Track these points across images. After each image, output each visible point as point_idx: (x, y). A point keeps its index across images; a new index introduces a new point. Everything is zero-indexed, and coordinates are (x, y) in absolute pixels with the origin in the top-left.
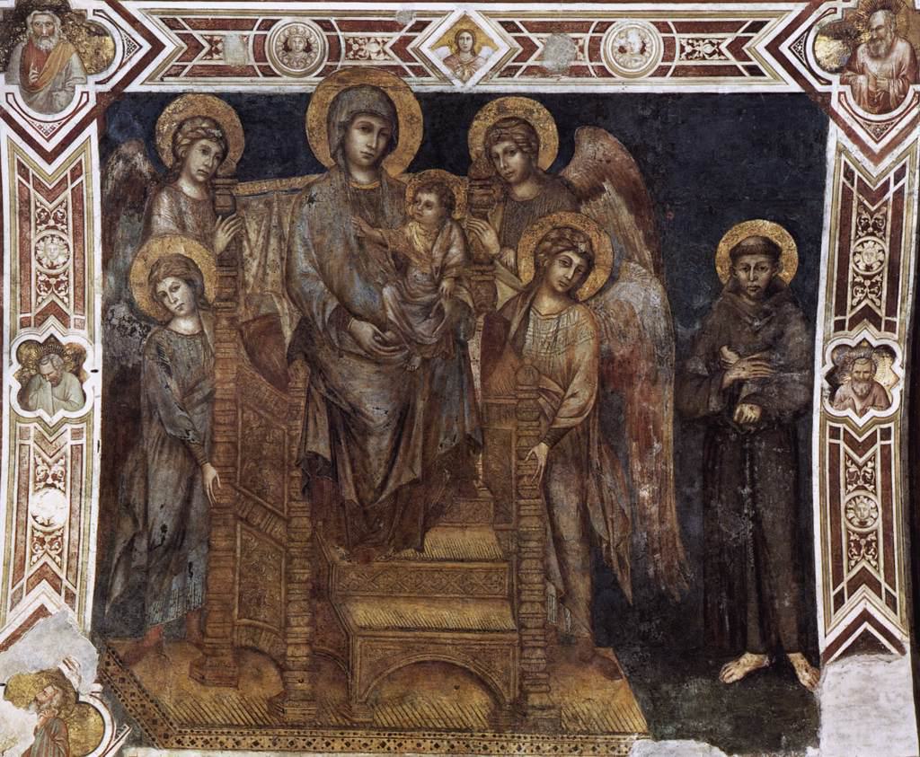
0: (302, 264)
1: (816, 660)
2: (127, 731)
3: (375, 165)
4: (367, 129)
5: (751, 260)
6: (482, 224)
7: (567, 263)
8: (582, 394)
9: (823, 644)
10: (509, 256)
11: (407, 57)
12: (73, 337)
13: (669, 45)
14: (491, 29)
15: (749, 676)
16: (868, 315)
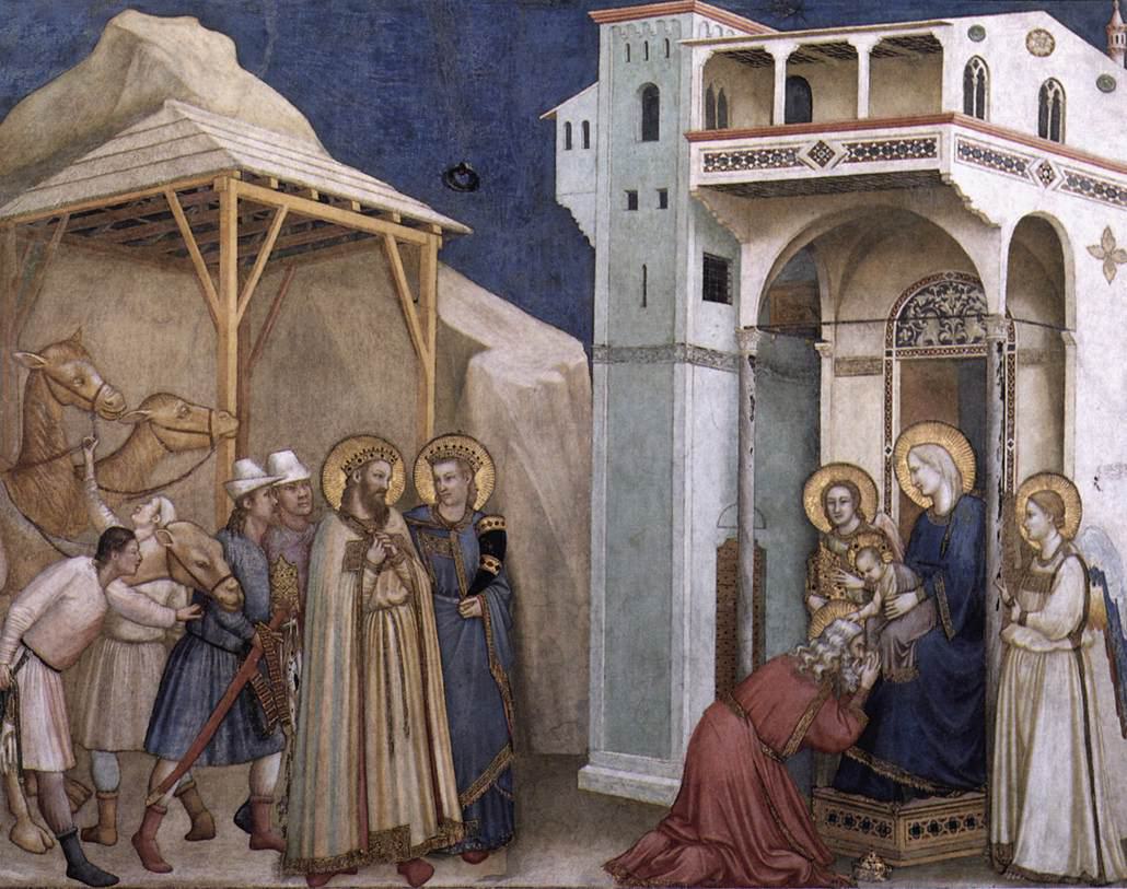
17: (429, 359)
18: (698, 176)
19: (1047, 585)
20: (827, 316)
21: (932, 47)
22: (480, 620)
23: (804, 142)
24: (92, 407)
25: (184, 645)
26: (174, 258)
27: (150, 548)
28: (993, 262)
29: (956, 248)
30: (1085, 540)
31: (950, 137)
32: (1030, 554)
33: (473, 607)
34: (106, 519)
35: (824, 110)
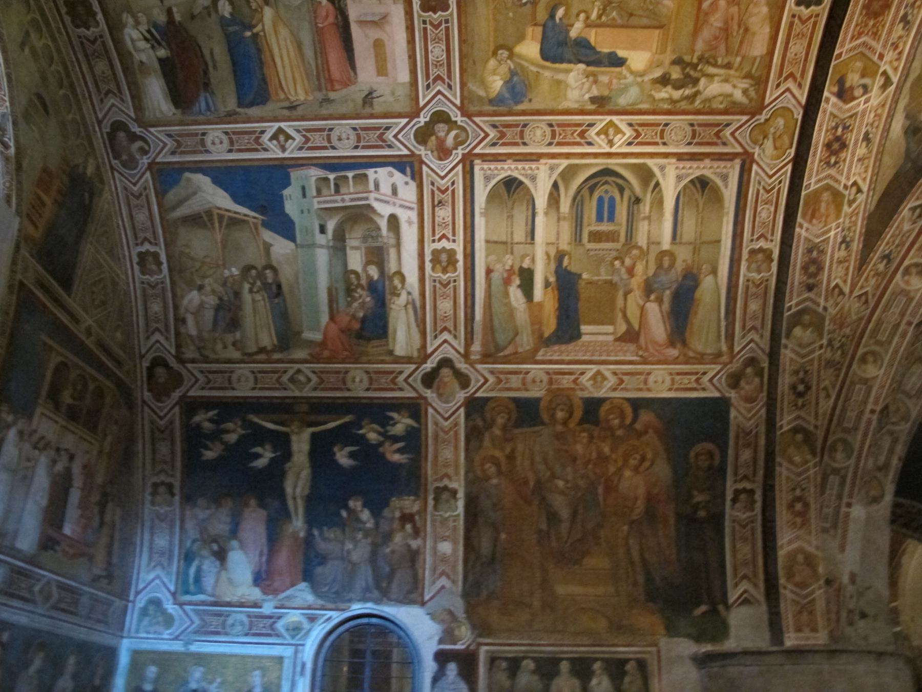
0: (538, 458)
1: (728, 607)
2: (476, 632)
3: (565, 423)
4: (562, 410)
5: (703, 457)
6: (603, 444)
7: (635, 459)
8: (640, 506)
9: (731, 601)
10: (614, 456)
11: (577, 384)
12: (453, 485)
13: (673, 380)
14: (608, 374)
15: (704, 614)
16: (745, 477)
17: (261, 247)
18: (316, 206)
19: (398, 295)
20: (347, 237)
21: (365, 176)
22: (278, 303)
23: (338, 198)
24: (192, 259)
25: (218, 308)
26: (203, 226)
27: (208, 288)
28: (383, 224)
29: (375, 223)
30: (407, 285)
31: (372, 196)
32: (395, 288)
33: (276, 301)
34: (199, 283)
35: (343, 190)
